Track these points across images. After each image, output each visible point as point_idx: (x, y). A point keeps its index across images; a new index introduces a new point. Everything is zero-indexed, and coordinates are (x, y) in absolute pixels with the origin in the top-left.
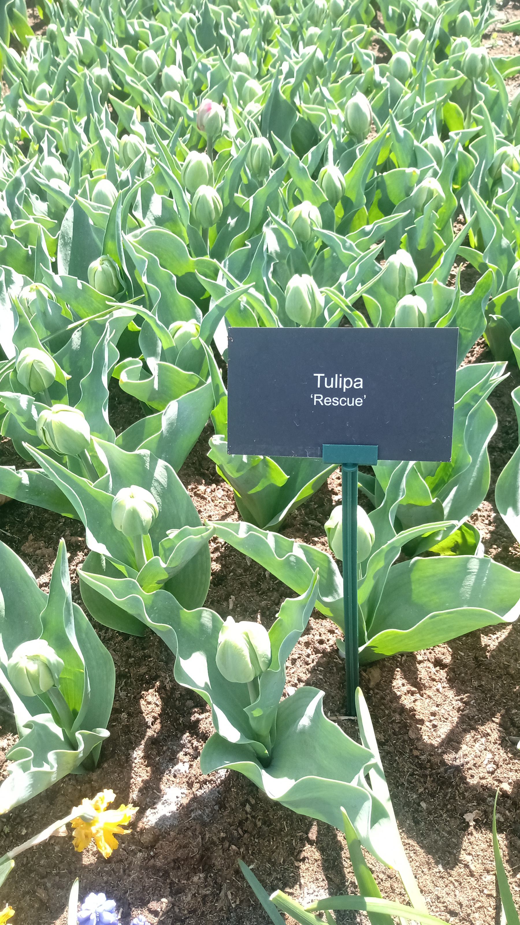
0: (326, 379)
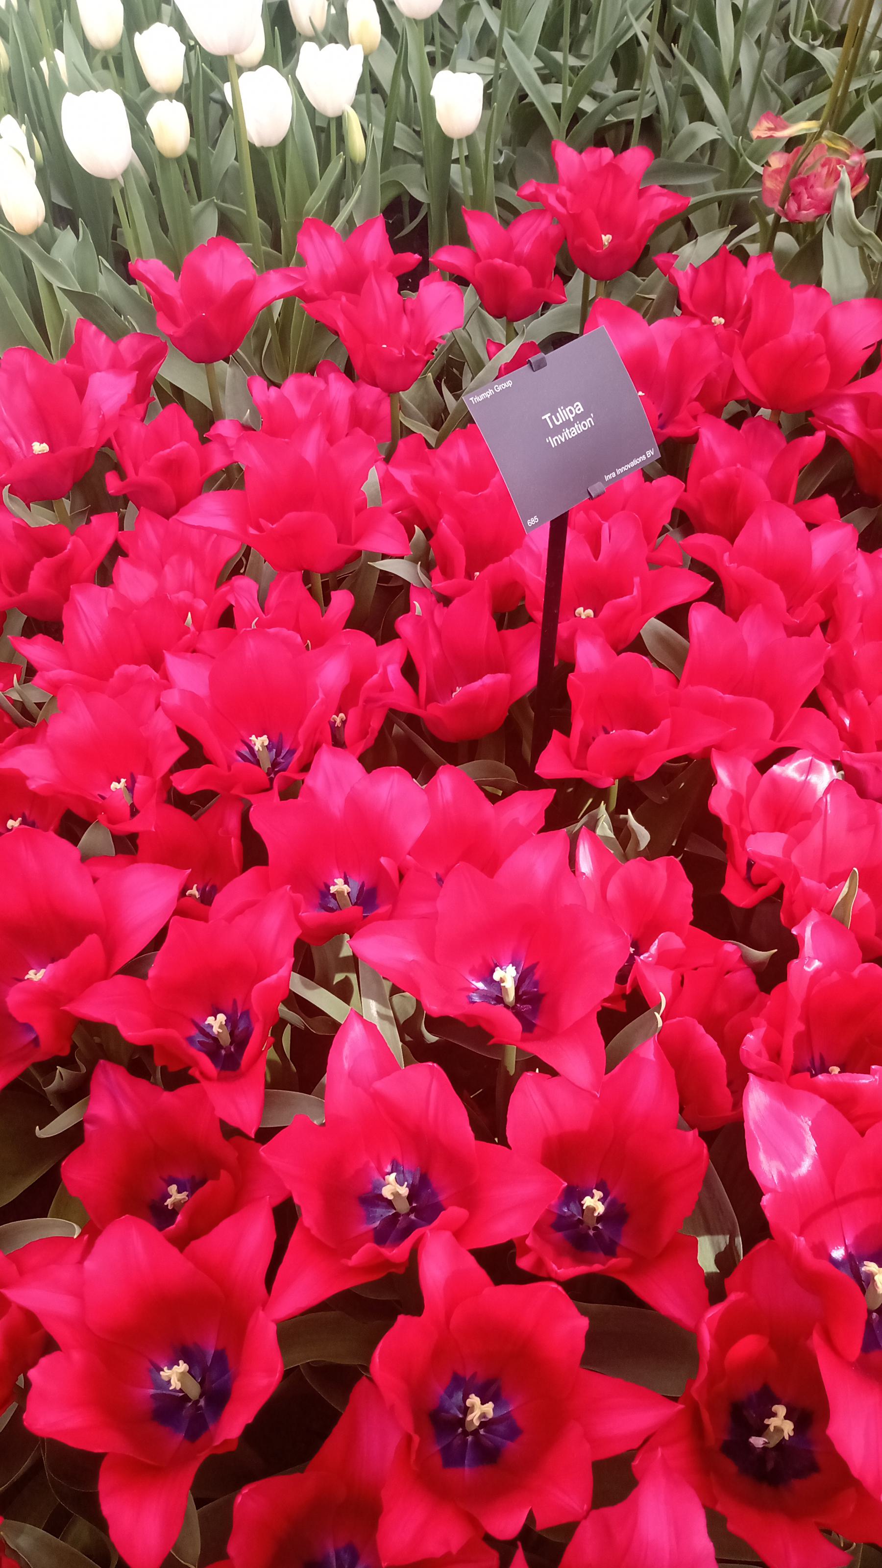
0: (553, 417)
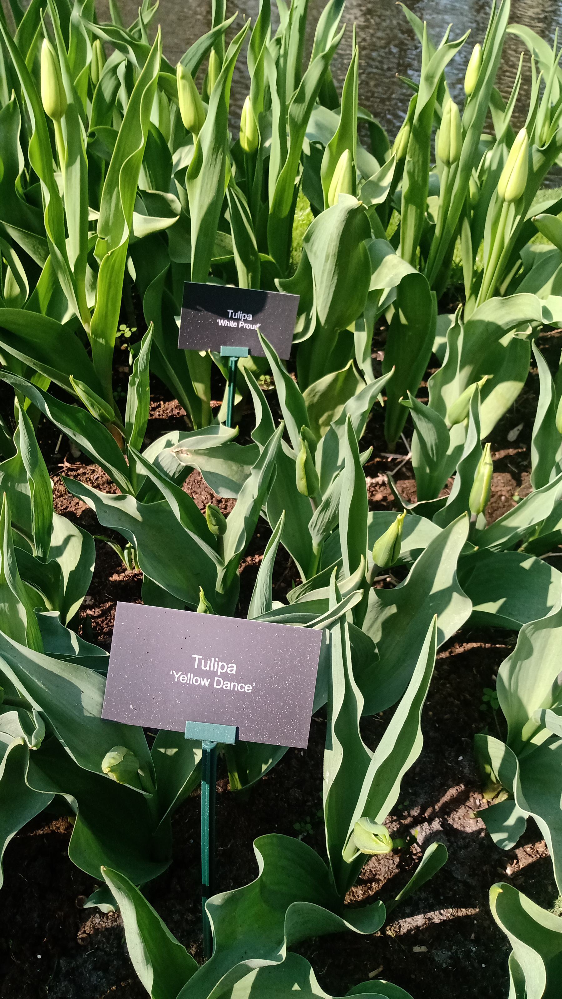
0: (203, 661)
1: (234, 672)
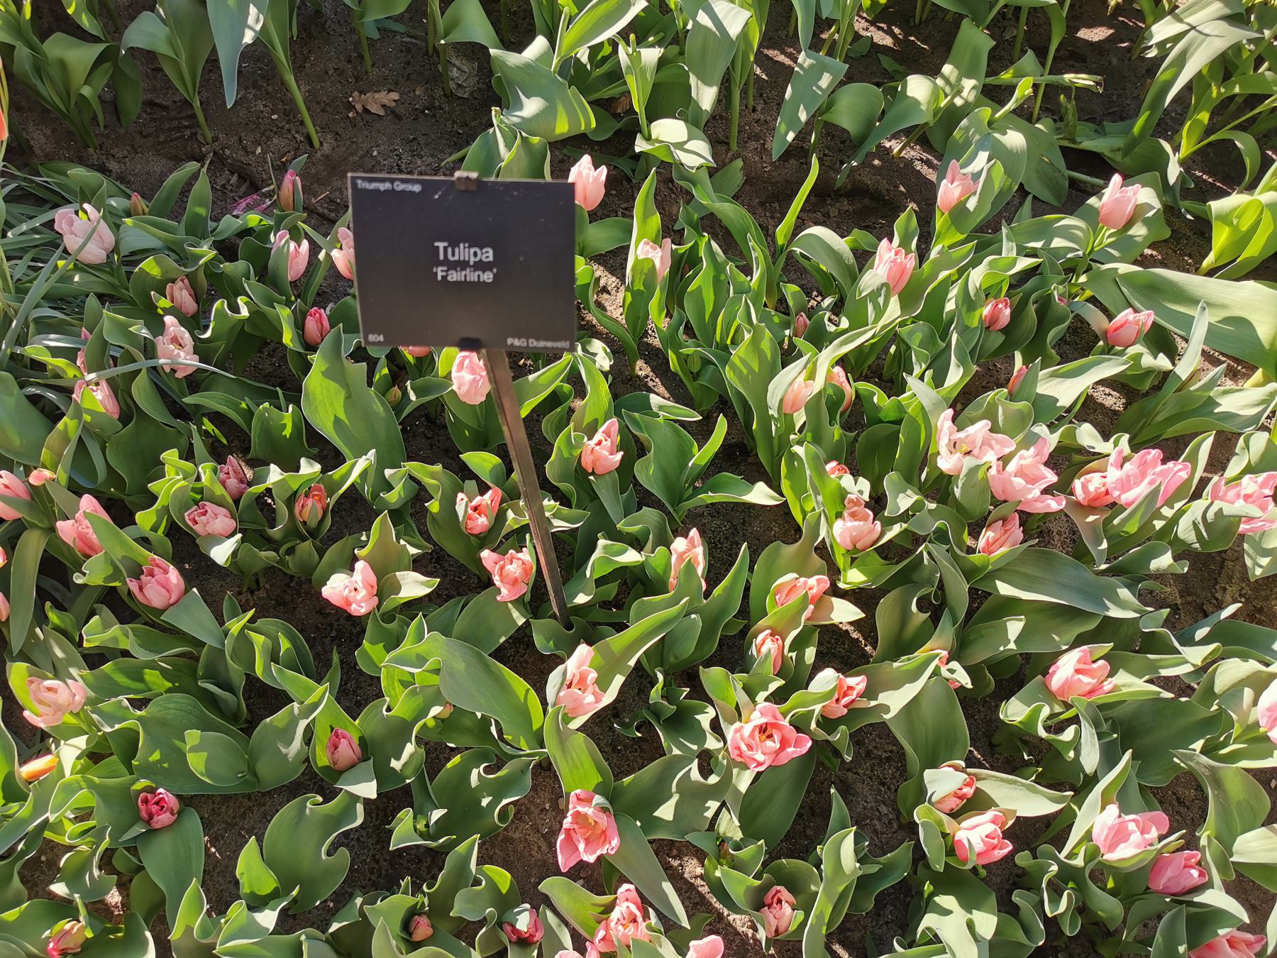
0: (450, 250)
1: (491, 259)
